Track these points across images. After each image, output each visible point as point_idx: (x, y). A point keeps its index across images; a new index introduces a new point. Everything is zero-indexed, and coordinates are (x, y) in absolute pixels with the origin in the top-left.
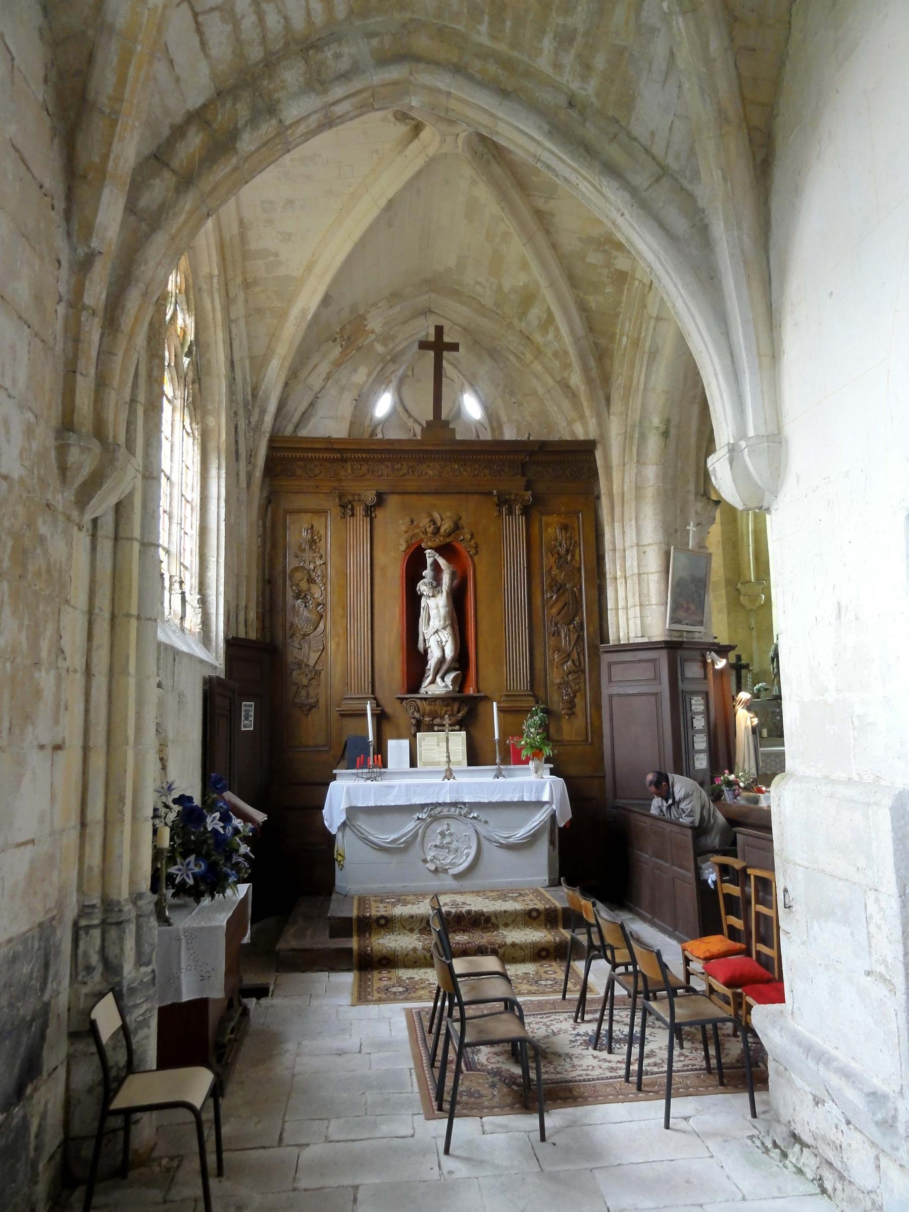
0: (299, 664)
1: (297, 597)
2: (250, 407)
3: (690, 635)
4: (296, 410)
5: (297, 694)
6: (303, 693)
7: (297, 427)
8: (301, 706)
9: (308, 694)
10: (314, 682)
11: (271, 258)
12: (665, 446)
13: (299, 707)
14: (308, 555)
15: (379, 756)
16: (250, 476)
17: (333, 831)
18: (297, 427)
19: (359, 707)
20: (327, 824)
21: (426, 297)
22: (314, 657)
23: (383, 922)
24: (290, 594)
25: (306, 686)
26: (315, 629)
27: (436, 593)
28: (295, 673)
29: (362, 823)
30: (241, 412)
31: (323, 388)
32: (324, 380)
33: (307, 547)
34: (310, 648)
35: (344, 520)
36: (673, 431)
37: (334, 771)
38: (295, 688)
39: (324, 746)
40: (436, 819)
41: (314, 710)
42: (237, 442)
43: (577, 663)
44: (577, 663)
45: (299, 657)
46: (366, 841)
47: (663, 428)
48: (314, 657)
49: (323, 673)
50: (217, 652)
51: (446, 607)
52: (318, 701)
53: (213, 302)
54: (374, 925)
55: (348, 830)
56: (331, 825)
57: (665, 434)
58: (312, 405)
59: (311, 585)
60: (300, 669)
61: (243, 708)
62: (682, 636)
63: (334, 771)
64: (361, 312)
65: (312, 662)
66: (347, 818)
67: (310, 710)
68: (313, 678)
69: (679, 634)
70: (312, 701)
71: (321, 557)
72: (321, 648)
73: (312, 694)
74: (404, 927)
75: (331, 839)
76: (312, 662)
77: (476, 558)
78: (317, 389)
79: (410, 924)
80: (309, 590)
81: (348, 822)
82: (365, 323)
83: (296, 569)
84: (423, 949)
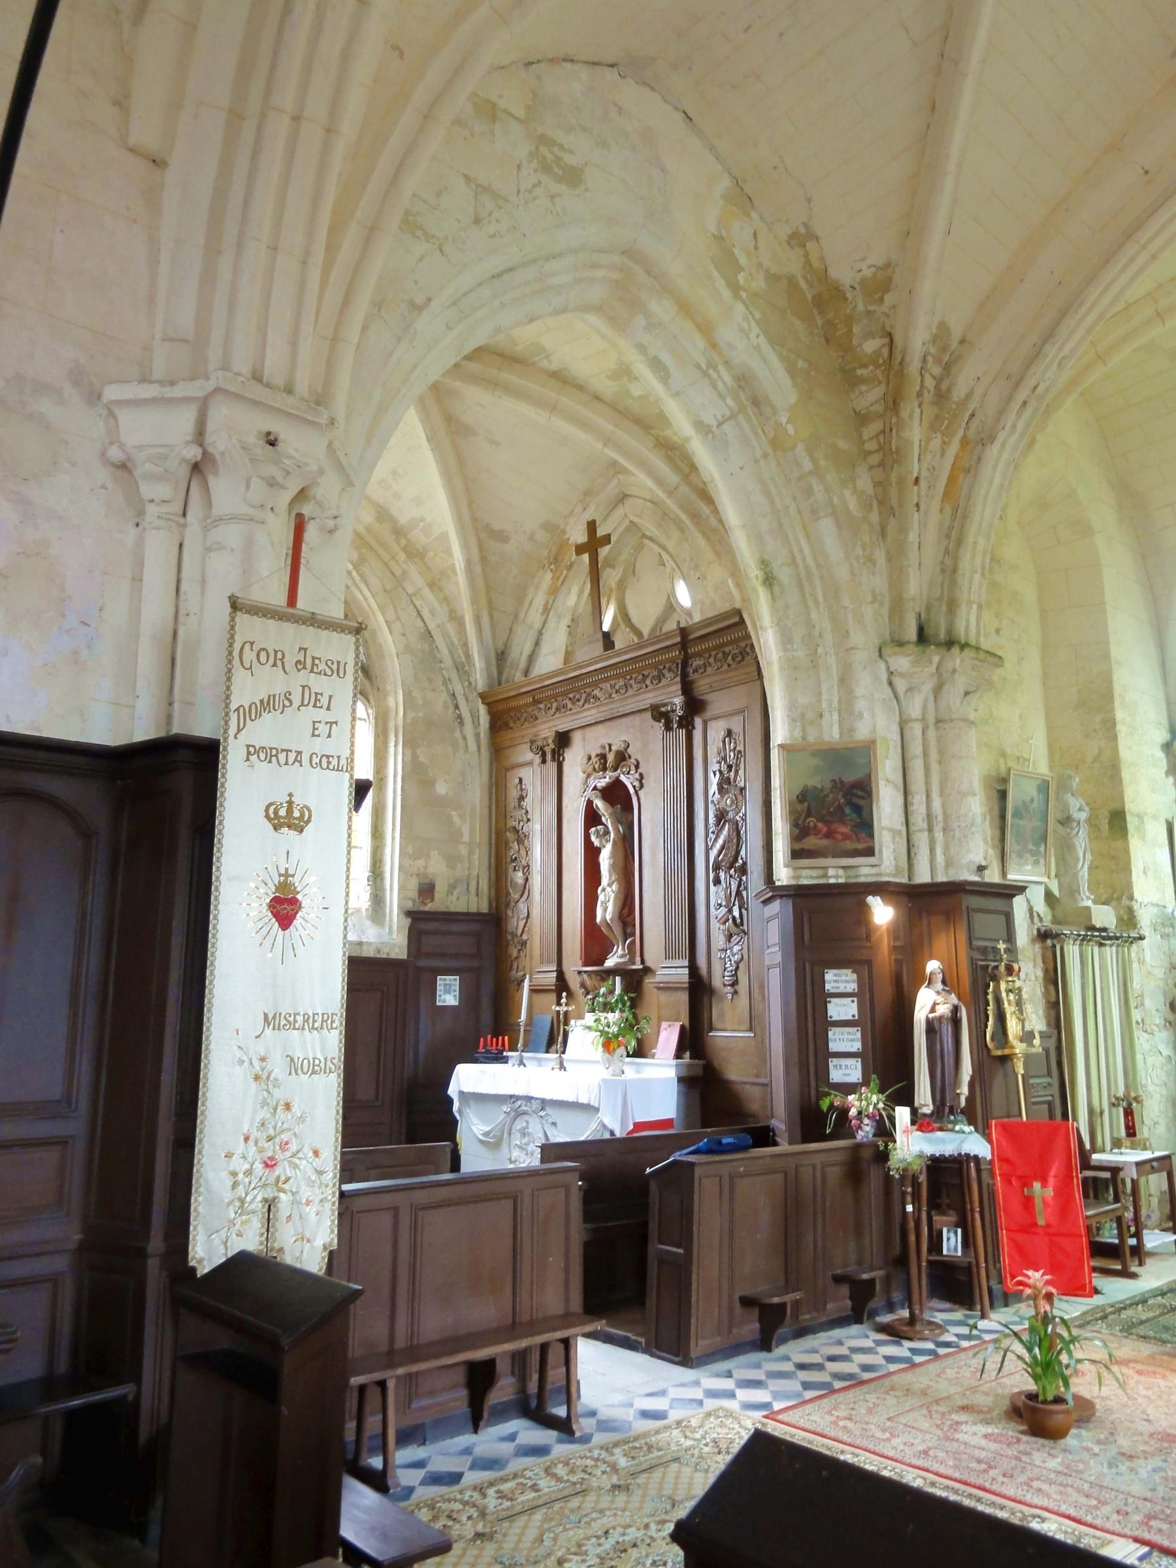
2: (466, 668)
3: (851, 872)
4: (521, 654)
7: (526, 673)
11: (422, 524)
12: (773, 599)
15: (506, 1038)
16: (477, 735)
18: (526, 673)
21: (615, 482)
27: (604, 842)
30: (454, 676)
31: (545, 623)
32: (542, 614)
36: (784, 574)
40: (519, 1114)
42: (457, 707)
43: (739, 921)
44: (739, 921)
47: (761, 574)
50: (391, 927)
51: (610, 858)
53: (361, 592)
57: (769, 581)
58: (537, 644)
61: (438, 982)
62: (825, 876)
64: (562, 527)
69: (820, 872)
77: (641, 793)
78: (537, 625)
82: (566, 537)
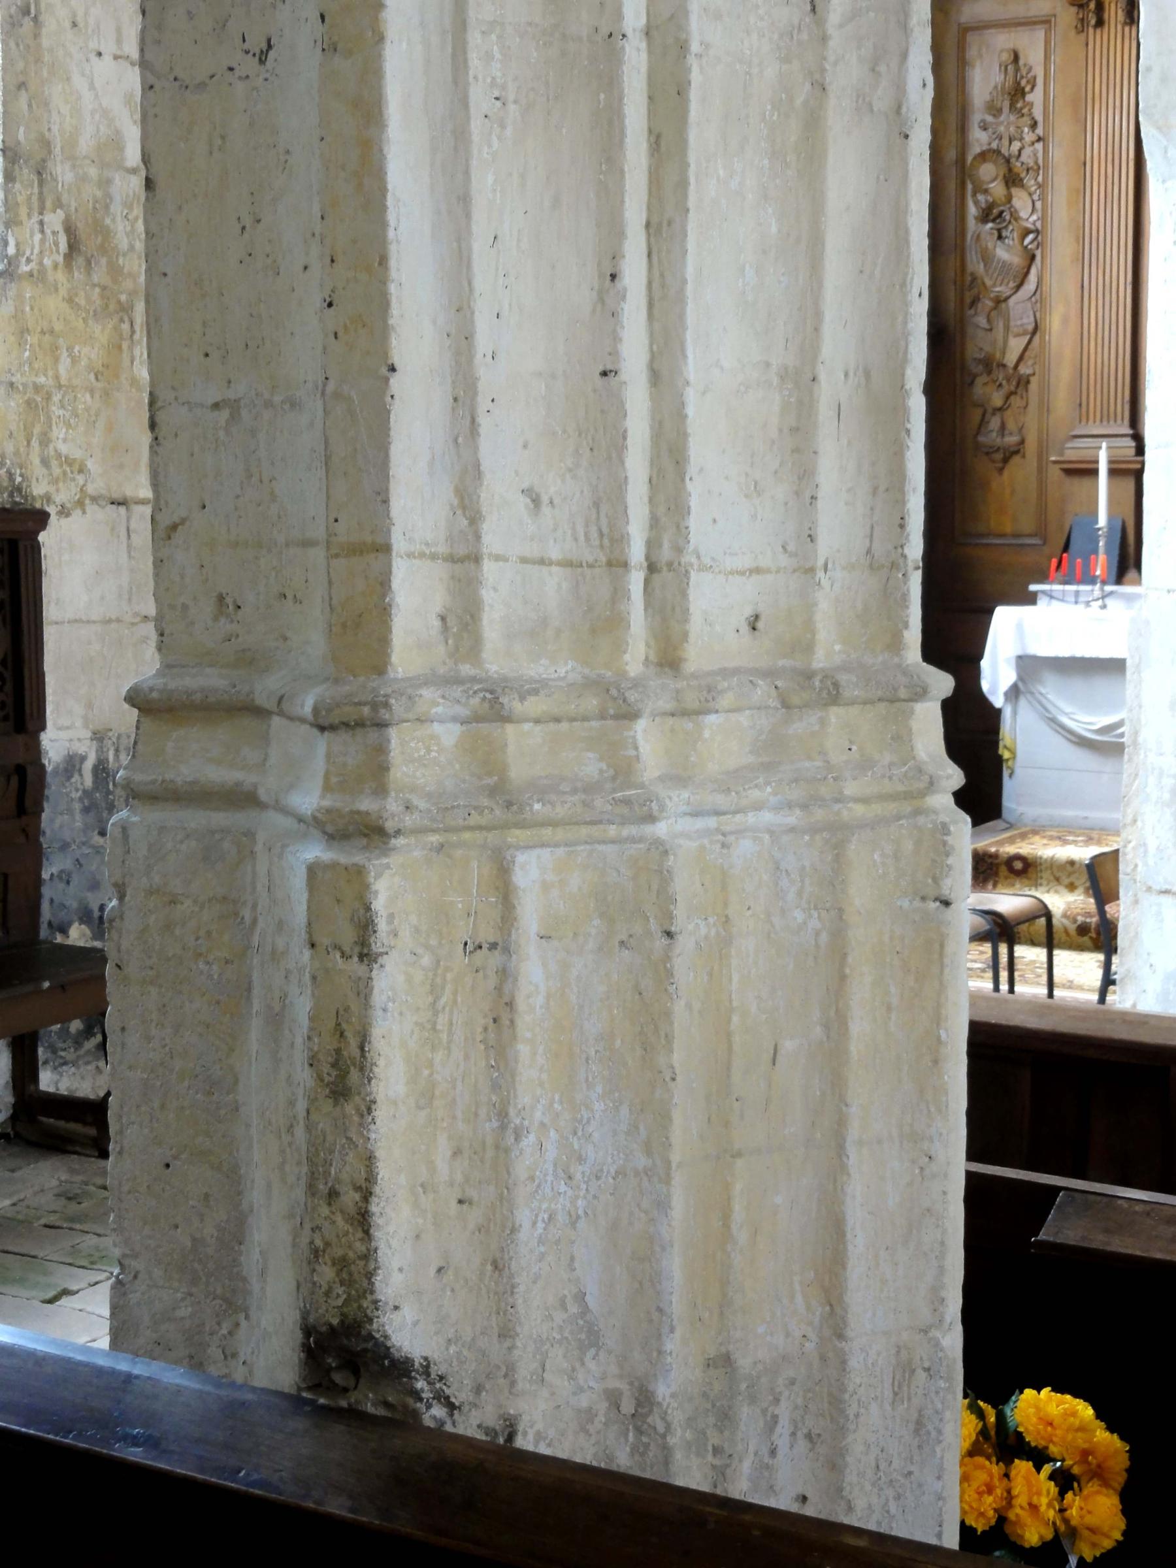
0: (989, 364)
1: (986, 215)
5: (983, 422)
6: (994, 423)
8: (990, 452)
9: (1003, 427)
10: (1016, 401)
13: (987, 454)
14: (1007, 122)
17: (998, 701)
19: (1086, 455)
20: (985, 686)
22: (1016, 345)
23: (1018, 865)
24: (972, 210)
25: (1000, 409)
26: (1018, 287)
28: (980, 381)
29: (1051, 690)
33: (1007, 104)
34: (1007, 328)
35: (1083, 36)
37: (1033, 588)
38: (979, 411)
39: (1030, 536)
41: (1016, 459)
45: (987, 348)
46: (1053, 722)
48: (1016, 345)
49: (1034, 381)
52: (1022, 442)
54: (1003, 870)
55: (1023, 702)
56: (994, 690)
59: (1014, 191)
60: (989, 372)
63: (1033, 588)
65: (1011, 358)
66: (1020, 678)
67: (1006, 460)
68: (1014, 393)
70: (1011, 440)
71: (1034, 125)
72: (1031, 327)
73: (1011, 425)
74: (1058, 879)
75: (992, 716)
76: (1011, 358)
79: (1069, 875)
80: (1009, 198)
81: (1020, 685)
83: (983, 156)
84: (1065, 915)
